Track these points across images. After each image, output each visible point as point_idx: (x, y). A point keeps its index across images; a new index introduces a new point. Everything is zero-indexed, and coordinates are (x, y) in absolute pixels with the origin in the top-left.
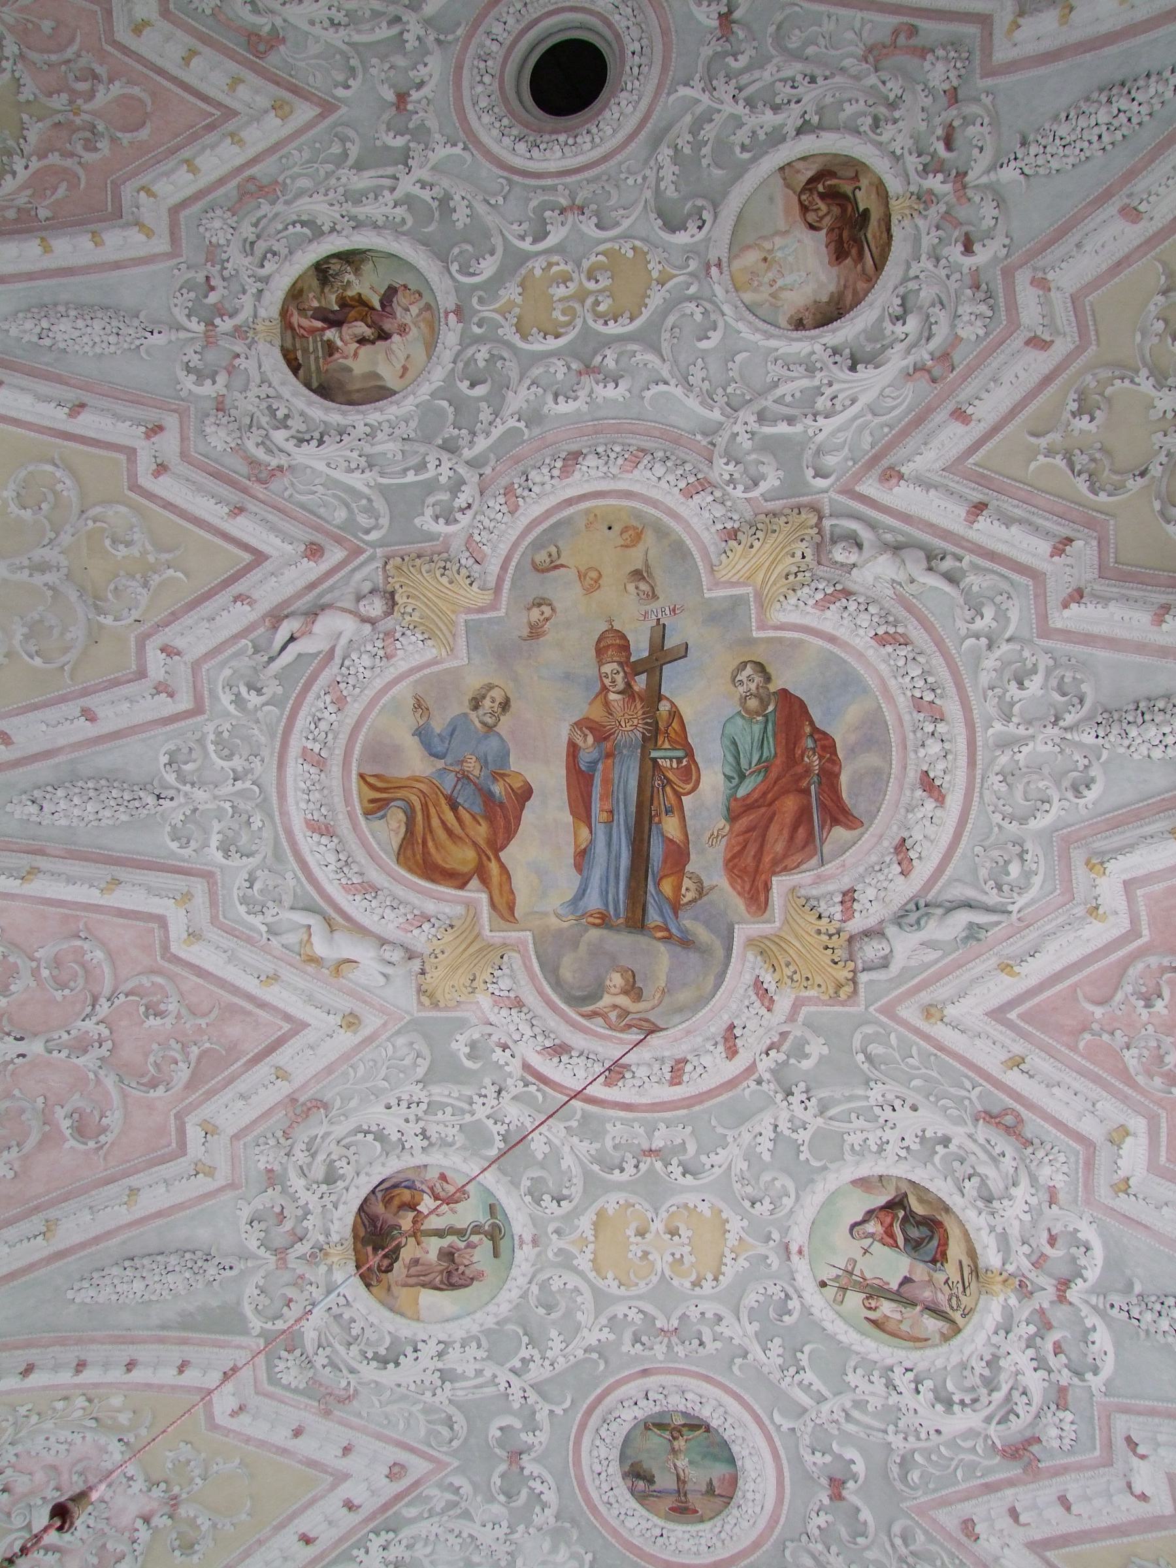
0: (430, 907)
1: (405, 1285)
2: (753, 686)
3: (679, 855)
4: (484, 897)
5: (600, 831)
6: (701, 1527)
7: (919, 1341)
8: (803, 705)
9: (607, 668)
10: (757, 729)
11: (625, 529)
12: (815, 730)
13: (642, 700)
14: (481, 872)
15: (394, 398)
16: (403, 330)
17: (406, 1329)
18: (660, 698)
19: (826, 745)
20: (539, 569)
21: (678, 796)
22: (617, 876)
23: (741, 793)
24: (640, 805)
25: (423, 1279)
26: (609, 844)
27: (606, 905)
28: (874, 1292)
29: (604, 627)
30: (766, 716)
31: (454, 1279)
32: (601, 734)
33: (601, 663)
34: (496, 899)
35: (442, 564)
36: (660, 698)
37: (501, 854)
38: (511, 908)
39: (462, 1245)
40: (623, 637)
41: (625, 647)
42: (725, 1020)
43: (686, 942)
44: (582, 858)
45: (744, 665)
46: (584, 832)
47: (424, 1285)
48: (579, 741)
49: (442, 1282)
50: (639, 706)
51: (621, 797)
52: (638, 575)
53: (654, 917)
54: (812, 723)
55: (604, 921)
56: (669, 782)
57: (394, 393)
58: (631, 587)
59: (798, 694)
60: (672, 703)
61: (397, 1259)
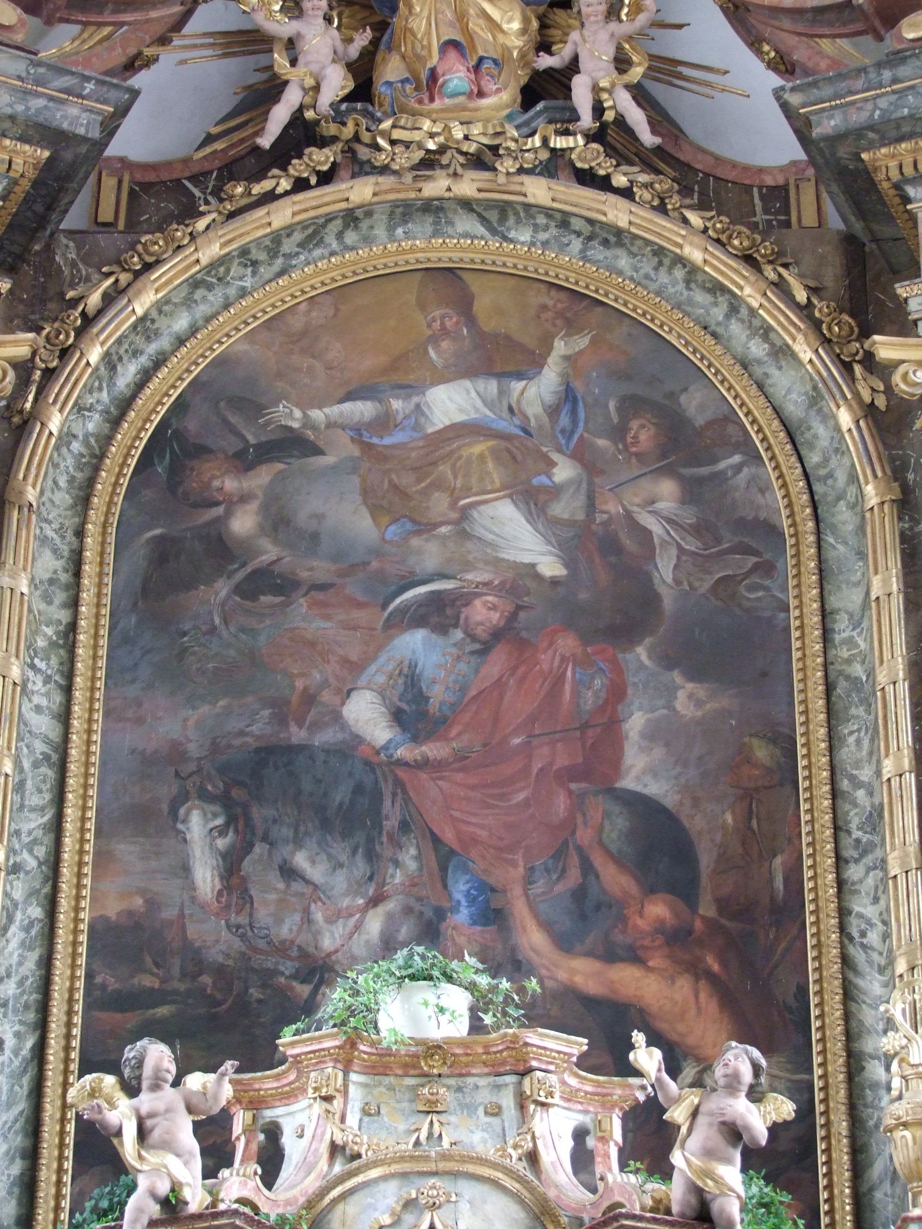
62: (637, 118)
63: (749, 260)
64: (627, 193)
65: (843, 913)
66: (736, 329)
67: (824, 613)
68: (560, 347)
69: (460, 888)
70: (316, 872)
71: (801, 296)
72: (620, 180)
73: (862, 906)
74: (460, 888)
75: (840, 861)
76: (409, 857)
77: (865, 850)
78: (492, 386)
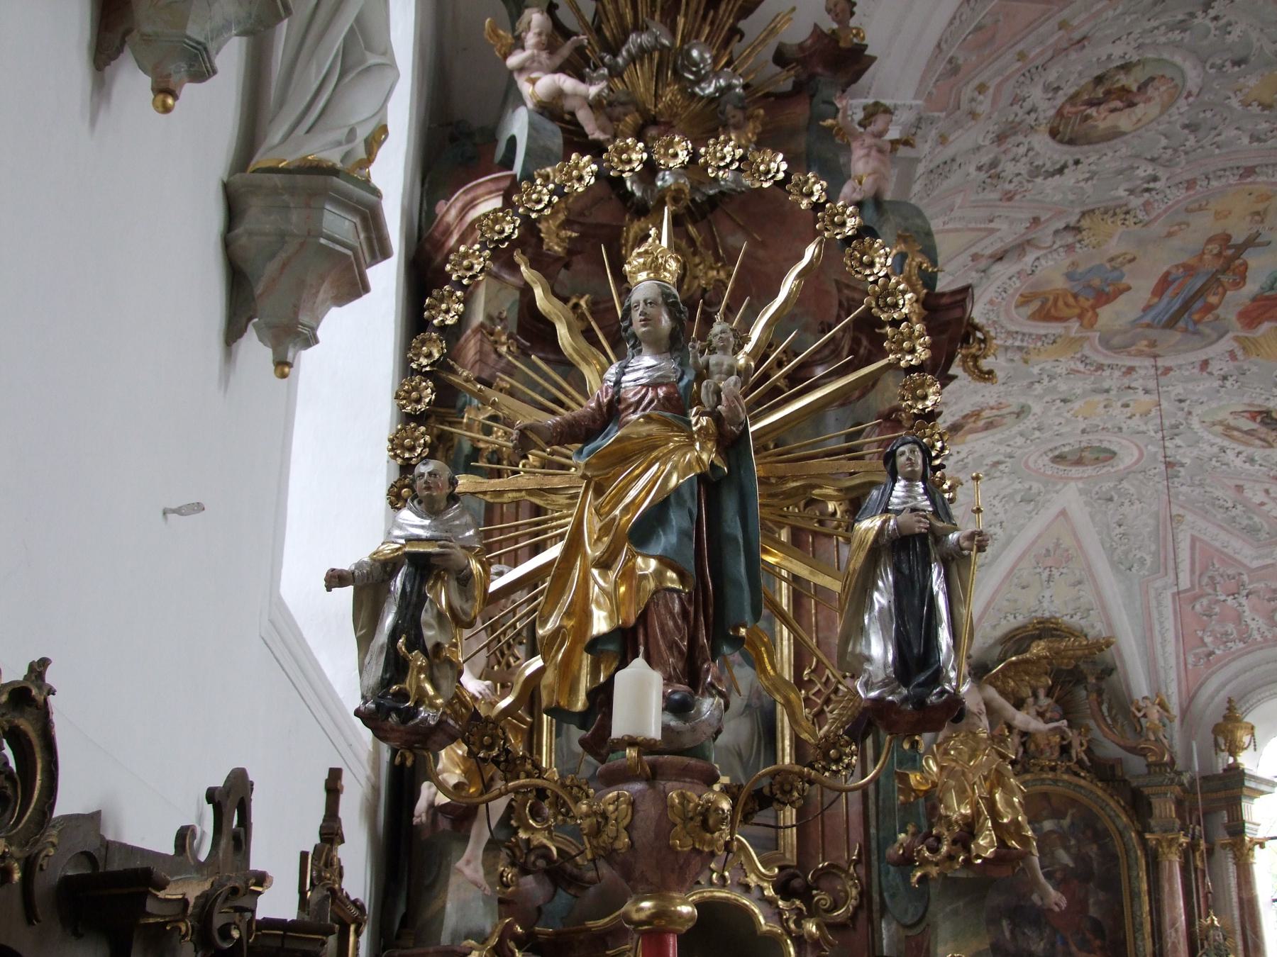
0: (1043, 332)
3: (1210, 308)
4: (1078, 324)
5: (1165, 299)
6: (1085, 468)
7: (1247, 444)
9: (1210, 247)
14: (1080, 317)
15: (1125, 138)
16: (1149, 100)
18: (1239, 258)
20: (1187, 210)
21: (1225, 291)
23: (1267, 294)
24: (1199, 290)
26: (1169, 303)
28: (1229, 427)
35: (1123, 216)
37: (1098, 310)
38: (1092, 326)
42: (1204, 357)
43: (1196, 333)
44: (1147, 308)
52: (1258, 213)
53: (1181, 324)
57: (1124, 134)
58: (1248, 218)
62: (1085, 758)
63: (1112, 796)
64: (1084, 778)
65: (1135, 944)
66: (1108, 808)
67: (1129, 877)
68: (1070, 812)
69: (1058, 937)
70: (1029, 933)
71: (1122, 803)
72: (1082, 774)
73: (1140, 943)
74: (1058, 937)
75: (1134, 932)
76: (1048, 931)
77: (1139, 930)
78: (1056, 821)
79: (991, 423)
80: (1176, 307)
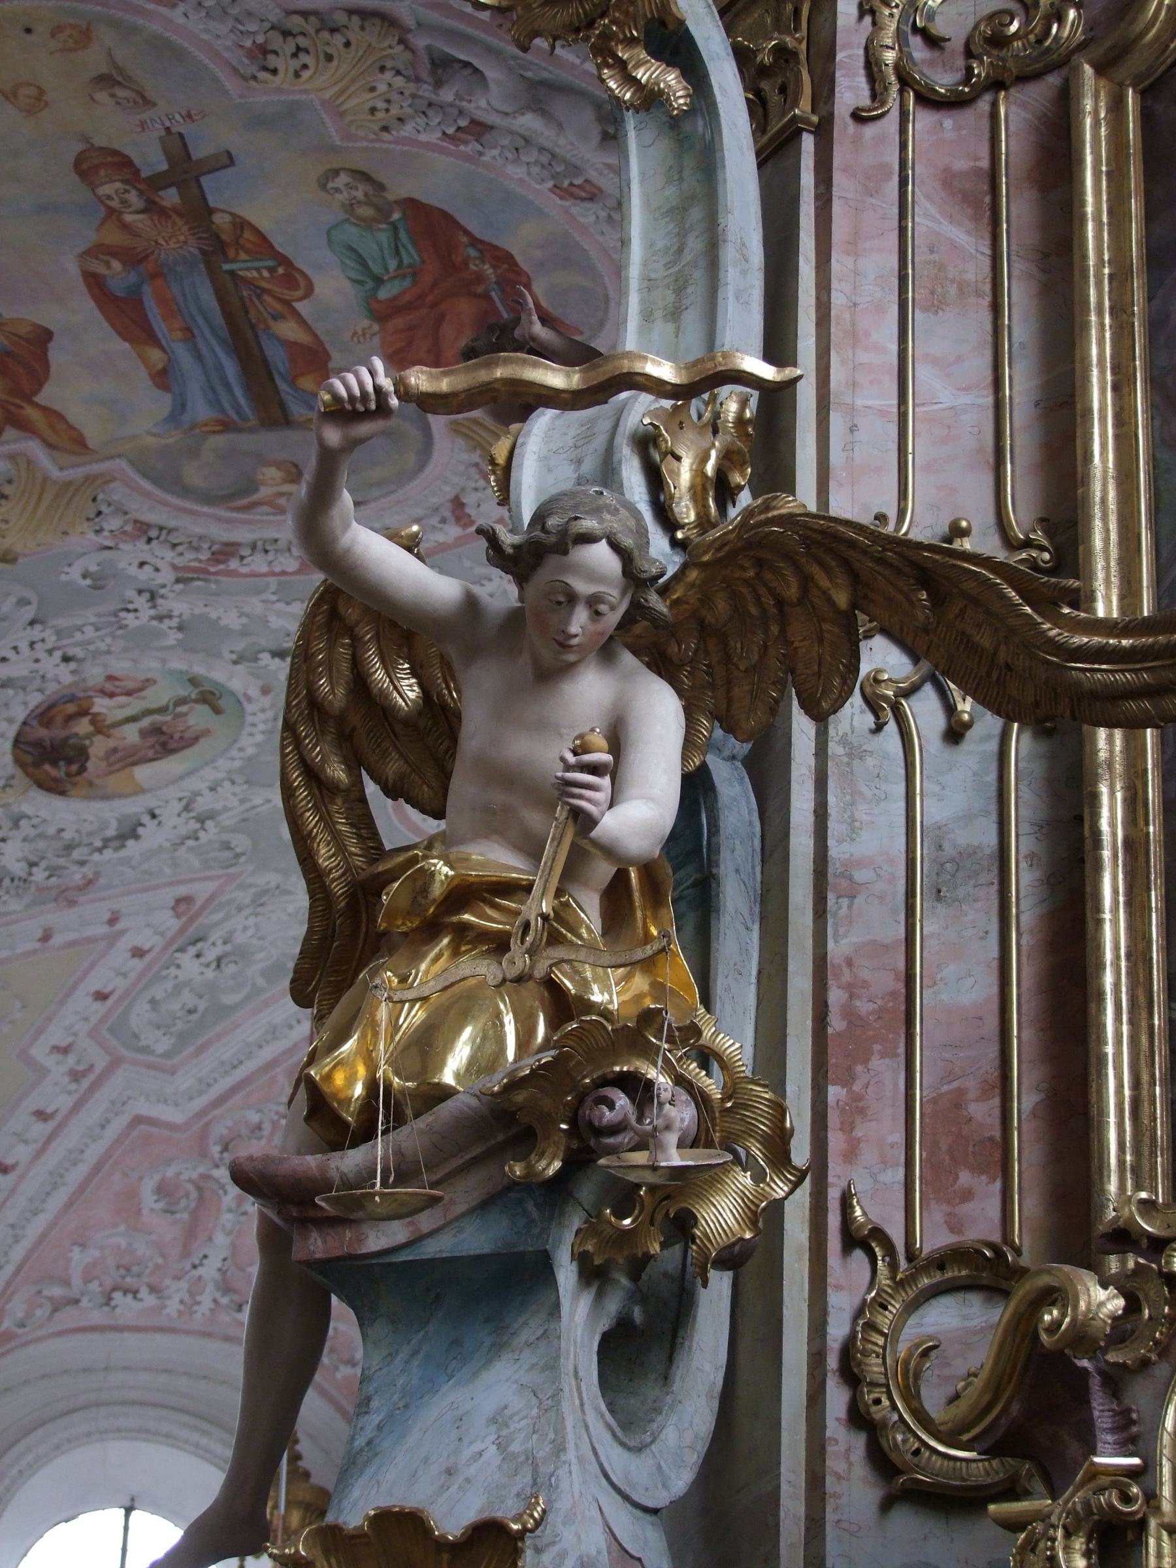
1: (110, 773)
2: (359, 194)
8: (445, 215)
10: (384, 237)
11: (55, 32)
12: (475, 242)
13: (180, 215)
17: (133, 807)
19: (502, 258)
21: (288, 304)
22: (227, 385)
24: (228, 316)
25: (129, 759)
26: (199, 357)
27: (222, 410)
29: (79, 147)
30: (395, 228)
31: (173, 745)
32: (133, 259)
33: (93, 188)
34: (52, 438)
36: (211, 211)
39: (168, 718)
40: (116, 153)
41: (123, 164)
42: (449, 492)
44: (163, 378)
45: (336, 172)
46: (155, 355)
47: (134, 764)
48: (101, 269)
49: (156, 753)
50: (180, 222)
51: (194, 311)
54: (467, 233)
55: (226, 426)
56: (264, 290)
59: (435, 202)
60: (232, 214)
61: (87, 758)
79: (157, 730)
80: (231, 369)
